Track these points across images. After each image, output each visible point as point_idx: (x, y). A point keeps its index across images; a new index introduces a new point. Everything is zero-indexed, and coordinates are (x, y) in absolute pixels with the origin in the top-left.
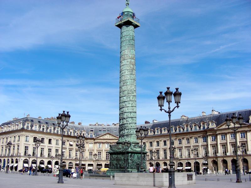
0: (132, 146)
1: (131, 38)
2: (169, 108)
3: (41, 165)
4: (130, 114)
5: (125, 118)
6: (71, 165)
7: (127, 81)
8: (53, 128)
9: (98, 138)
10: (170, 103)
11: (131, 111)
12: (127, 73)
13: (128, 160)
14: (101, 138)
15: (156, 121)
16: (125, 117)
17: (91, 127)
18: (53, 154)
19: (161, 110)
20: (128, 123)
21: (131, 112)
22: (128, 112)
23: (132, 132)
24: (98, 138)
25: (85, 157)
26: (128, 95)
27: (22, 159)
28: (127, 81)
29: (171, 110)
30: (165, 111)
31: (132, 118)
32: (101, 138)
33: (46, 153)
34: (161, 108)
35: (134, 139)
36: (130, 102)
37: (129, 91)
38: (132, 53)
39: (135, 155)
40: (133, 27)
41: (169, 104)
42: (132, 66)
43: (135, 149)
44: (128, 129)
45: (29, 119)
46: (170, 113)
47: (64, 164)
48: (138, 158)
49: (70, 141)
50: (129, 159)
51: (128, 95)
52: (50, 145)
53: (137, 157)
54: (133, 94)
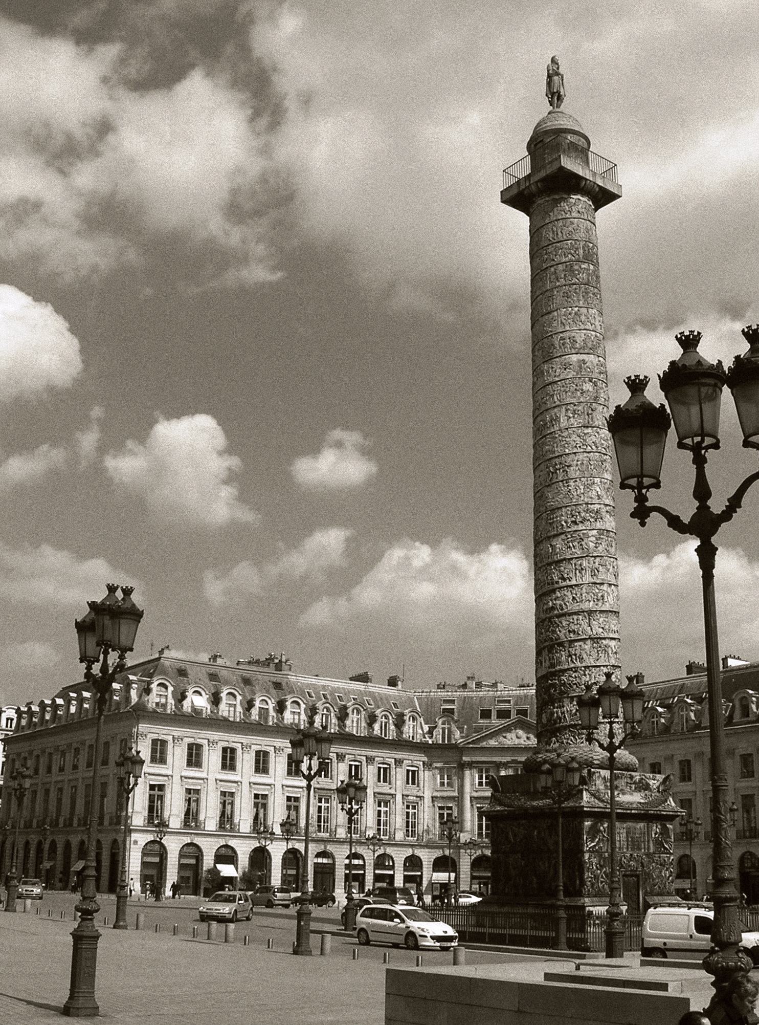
1: (581, 252)
2: (702, 491)
3: (219, 867)
4: (584, 624)
5: (561, 644)
6: (357, 867)
7: (569, 459)
8: (271, 706)
9: (484, 744)
10: (710, 454)
11: (591, 605)
12: (563, 423)
13: (583, 852)
14: (493, 743)
15: (739, 658)
16: (562, 634)
17: (443, 694)
18: (277, 814)
19: (641, 513)
20: (578, 664)
21: (590, 612)
22: (577, 613)
24: (484, 744)
25: (420, 829)
26: (575, 528)
27: (136, 842)
28: (569, 459)
29: (717, 505)
30: (674, 522)
31: (596, 639)
32: (493, 743)
33: (244, 818)
34: (641, 499)
36: (585, 563)
37: (580, 509)
38: (591, 328)
41: (700, 462)
42: (588, 386)
45: (167, 663)
46: (714, 531)
47: (325, 861)
48: (634, 844)
49: (347, 756)
50: (586, 849)
51: (575, 528)
52: (261, 779)
53: (625, 835)
54: (599, 525)
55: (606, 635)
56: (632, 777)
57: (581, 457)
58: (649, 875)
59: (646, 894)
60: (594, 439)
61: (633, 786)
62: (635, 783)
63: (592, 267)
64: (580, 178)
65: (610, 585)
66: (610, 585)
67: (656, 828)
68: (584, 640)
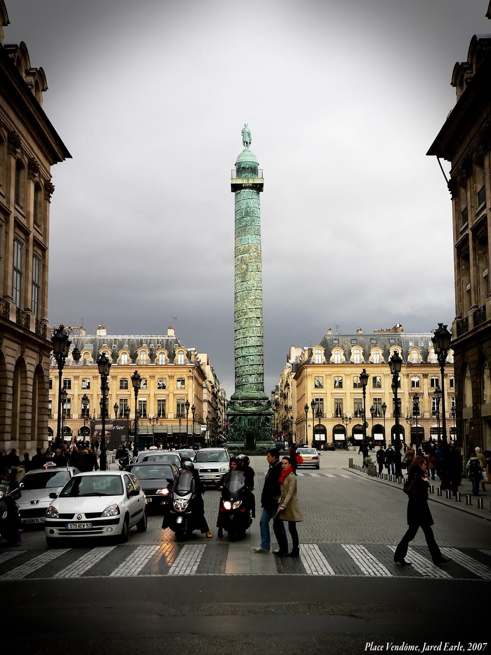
0: (237, 405)
1: (244, 214)
11: (242, 345)
21: (242, 348)
22: (238, 348)
23: (244, 380)
31: (244, 357)
35: (247, 392)
36: (241, 330)
39: (243, 417)
40: (247, 190)
42: (244, 266)
43: (242, 409)
44: (239, 376)
48: (251, 423)
49: (429, 375)
53: (247, 421)
54: (246, 317)
55: (248, 355)
56: (253, 402)
57: (241, 293)
58: (258, 434)
59: (257, 440)
60: (245, 286)
61: (253, 405)
62: (254, 404)
63: (248, 218)
64: (242, 184)
65: (250, 337)
66: (250, 337)
67: (263, 418)
68: (240, 357)
